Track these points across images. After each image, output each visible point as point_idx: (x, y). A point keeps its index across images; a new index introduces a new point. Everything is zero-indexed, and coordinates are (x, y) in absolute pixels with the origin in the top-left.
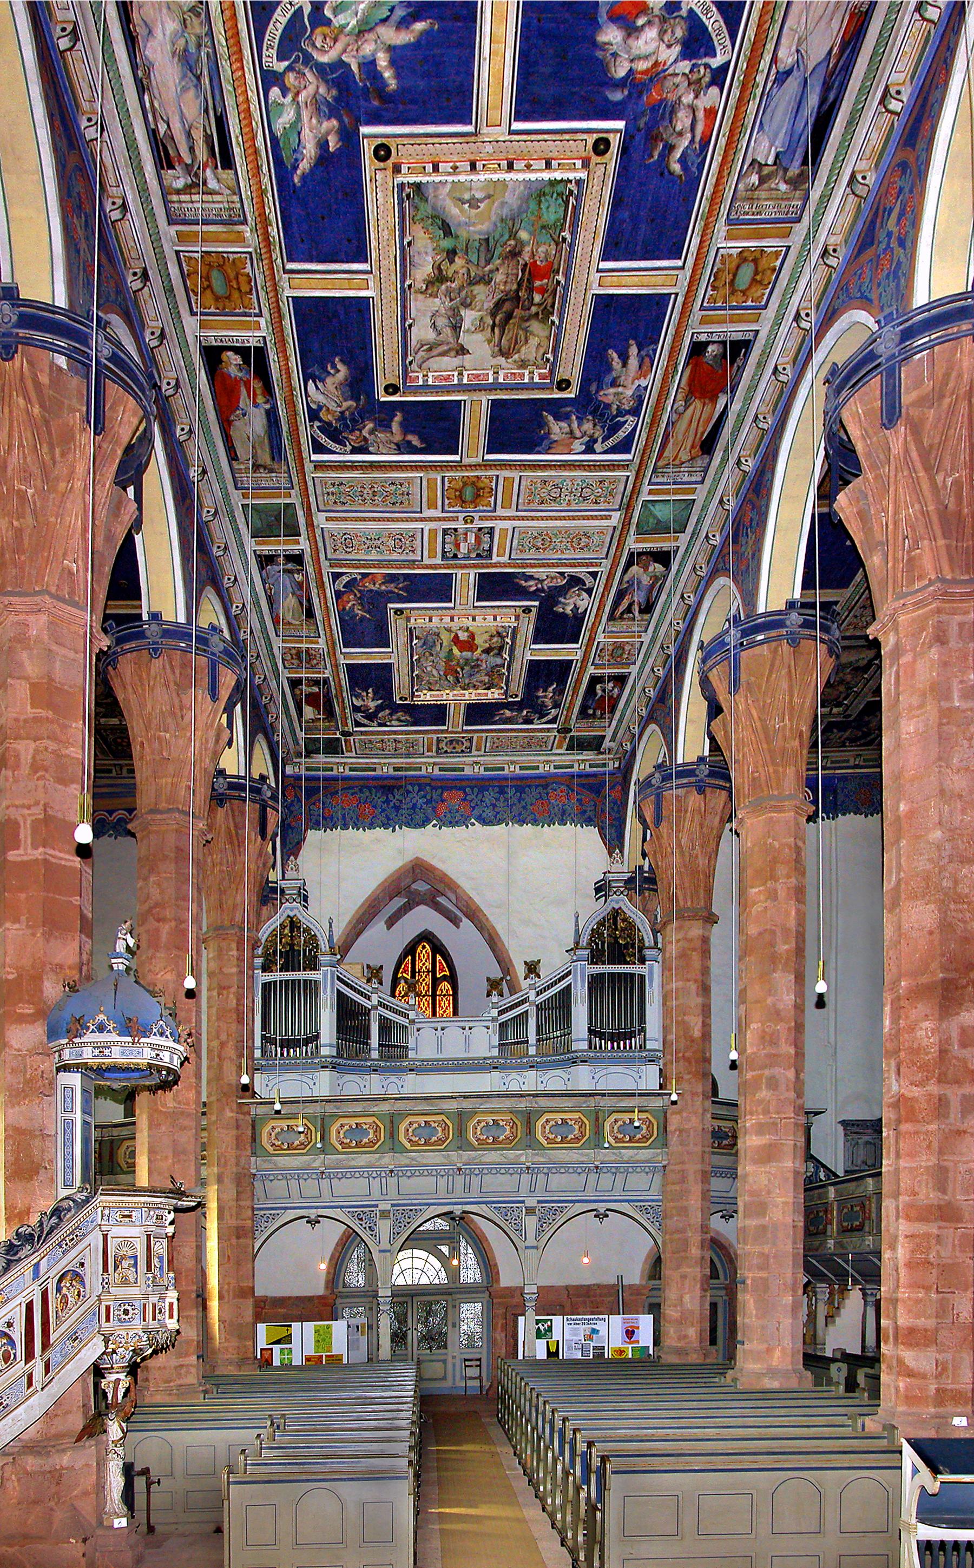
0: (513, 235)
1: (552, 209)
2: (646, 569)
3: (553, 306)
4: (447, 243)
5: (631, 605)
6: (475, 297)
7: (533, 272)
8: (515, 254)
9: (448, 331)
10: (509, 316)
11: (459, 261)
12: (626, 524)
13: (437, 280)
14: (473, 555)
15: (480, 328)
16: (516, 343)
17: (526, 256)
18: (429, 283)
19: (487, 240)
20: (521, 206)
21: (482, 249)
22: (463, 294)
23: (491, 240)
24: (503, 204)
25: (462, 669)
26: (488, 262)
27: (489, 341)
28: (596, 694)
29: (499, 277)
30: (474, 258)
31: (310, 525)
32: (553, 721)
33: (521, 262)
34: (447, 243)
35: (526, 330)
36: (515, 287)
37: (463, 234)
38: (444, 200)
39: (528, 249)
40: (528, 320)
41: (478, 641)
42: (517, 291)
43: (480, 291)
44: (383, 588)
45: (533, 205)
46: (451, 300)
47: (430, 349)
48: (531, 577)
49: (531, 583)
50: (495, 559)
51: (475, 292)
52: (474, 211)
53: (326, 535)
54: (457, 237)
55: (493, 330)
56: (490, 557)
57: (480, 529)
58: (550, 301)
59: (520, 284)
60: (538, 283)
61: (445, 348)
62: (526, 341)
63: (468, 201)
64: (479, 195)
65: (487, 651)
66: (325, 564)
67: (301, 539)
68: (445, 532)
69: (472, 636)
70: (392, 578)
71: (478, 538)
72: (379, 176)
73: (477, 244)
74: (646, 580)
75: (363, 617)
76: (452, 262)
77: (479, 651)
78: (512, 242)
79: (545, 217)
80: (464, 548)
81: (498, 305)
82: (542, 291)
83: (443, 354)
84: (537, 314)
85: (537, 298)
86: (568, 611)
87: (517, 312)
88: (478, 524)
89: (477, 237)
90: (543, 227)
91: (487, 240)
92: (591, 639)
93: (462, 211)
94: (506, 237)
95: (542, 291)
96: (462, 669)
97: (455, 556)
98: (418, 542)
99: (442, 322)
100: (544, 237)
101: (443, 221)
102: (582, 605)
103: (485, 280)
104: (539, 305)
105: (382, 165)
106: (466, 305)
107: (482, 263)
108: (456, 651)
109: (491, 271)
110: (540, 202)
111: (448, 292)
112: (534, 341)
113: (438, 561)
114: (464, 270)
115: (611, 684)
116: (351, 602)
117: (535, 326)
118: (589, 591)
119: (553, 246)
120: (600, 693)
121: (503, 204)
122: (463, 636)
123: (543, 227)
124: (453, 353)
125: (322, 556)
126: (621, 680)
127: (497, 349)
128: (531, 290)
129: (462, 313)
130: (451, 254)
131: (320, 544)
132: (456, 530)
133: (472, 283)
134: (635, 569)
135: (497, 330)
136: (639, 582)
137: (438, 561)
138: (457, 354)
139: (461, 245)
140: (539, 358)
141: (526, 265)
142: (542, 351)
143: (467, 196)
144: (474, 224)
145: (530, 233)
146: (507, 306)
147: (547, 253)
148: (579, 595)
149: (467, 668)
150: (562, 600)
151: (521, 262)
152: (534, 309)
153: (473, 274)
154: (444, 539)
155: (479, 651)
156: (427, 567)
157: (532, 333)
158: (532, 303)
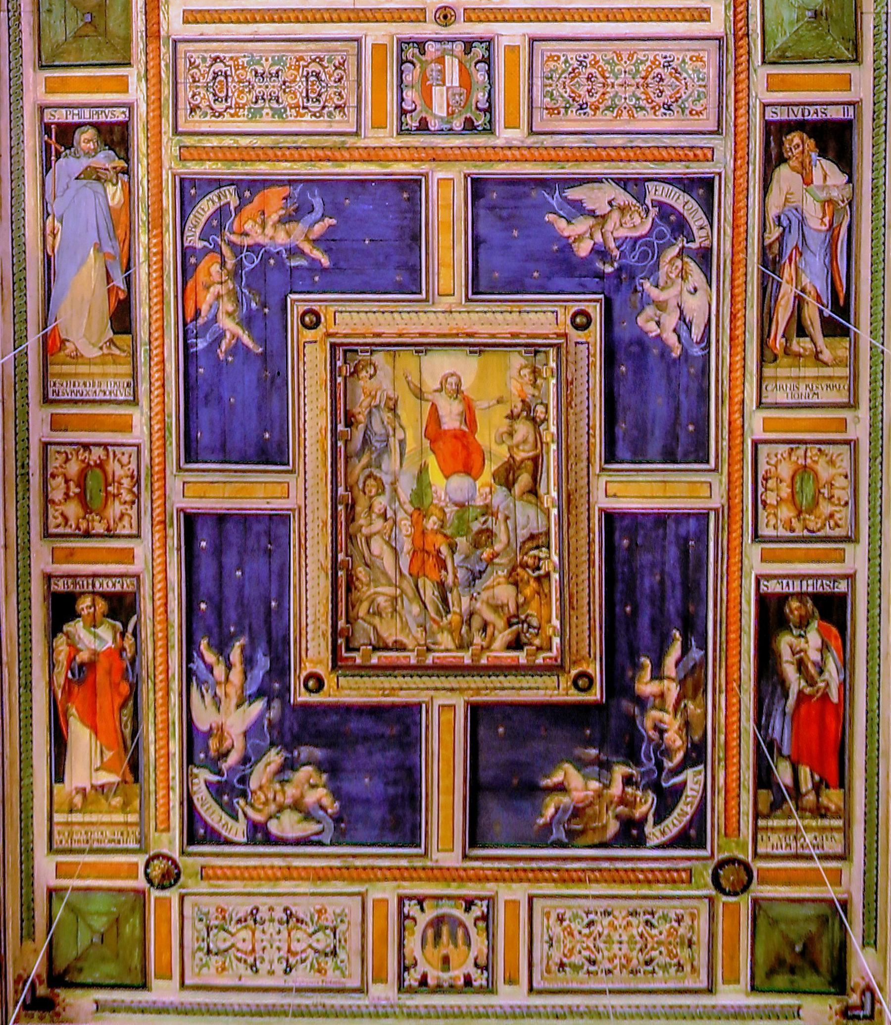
2: (808, 182)
5: (799, 302)
12: (741, 34)
14: (458, 124)
25: (453, 548)
28: (783, 683)
31: (153, 34)
32: (691, 836)
41: (485, 437)
44: (281, 238)
48: (578, 208)
49: (582, 225)
50: (505, 135)
53: (181, 63)
56: (489, 130)
57: (468, 45)
65: (507, 476)
66: (170, 147)
67: (133, 74)
68: (403, 43)
69: (469, 416)
70: (300, 200)
71: (464, 73)
74: (816, 221)
75: (238, 348)
77: (486, 476)
80: (439, 108)
86: (671, 339)
88: (462, 29)
92: (737, 430)
96: (453, 548)
97: (423, 127)
98: (349, 83)
102: (695, 306)
108: (435, 474)
113: (388, 137)
115: (814, 638)
116: (215, 294)
118: (704, 257)
120: (790, 671)
122: (451, 420)
125: (167, 126)
126: (832, 608)
131: (167, 91)
132: (421, 44)
134: (785, 175)
136: (802, 222)
137: (388, 137)
148: (683, 275)
149: (462, 542)
150: (654, 293)
154: (401, 73)
155: (486, 476)
156: (370, 155)
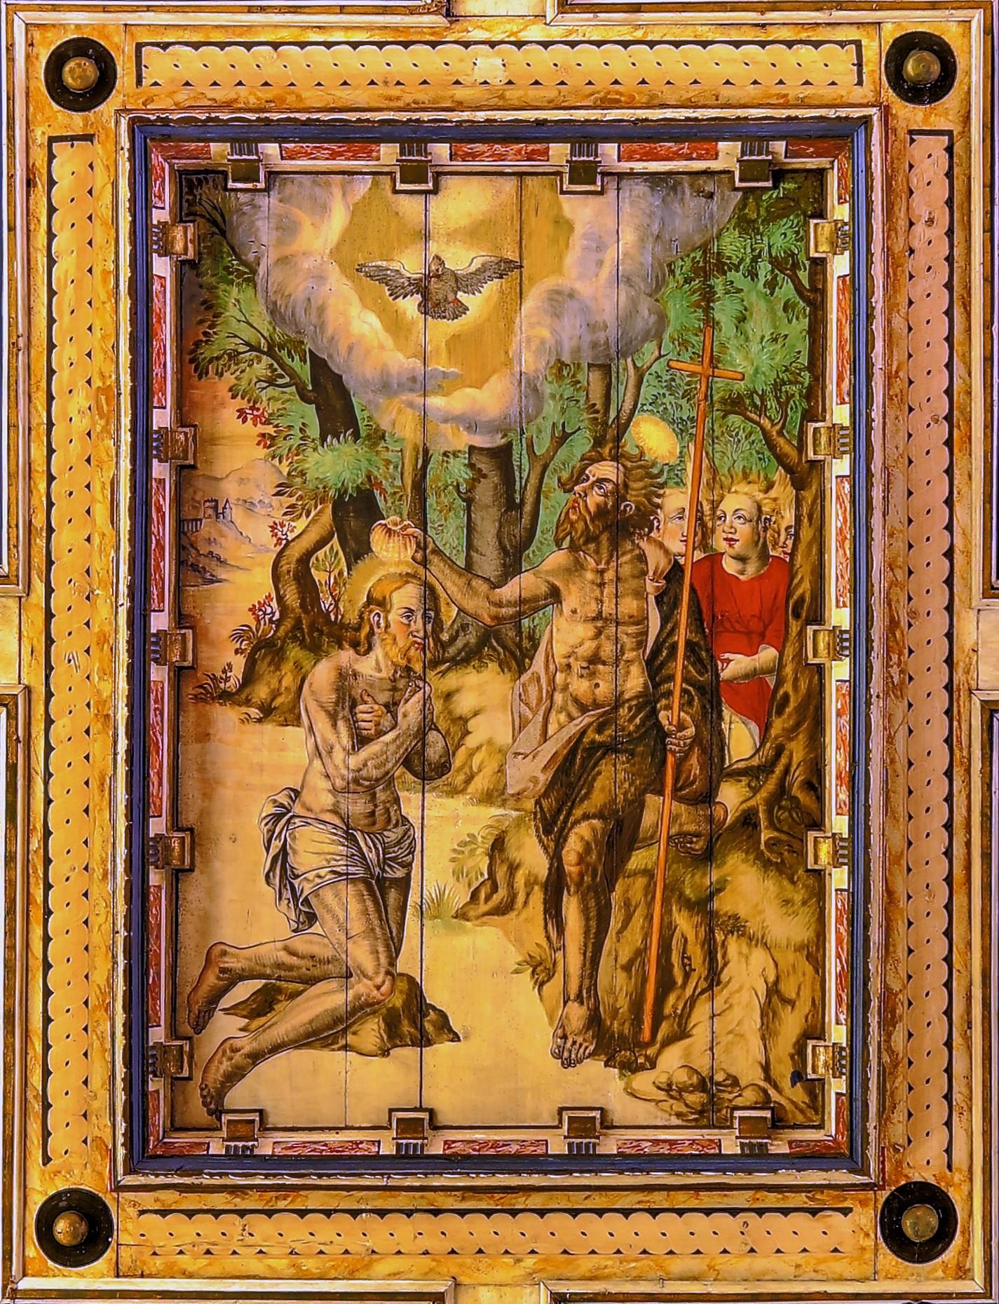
0: (610, 436)
1: (759, 325)
3: (815, 784)
4: (334, 464)
6: (464, 720)
7: (703, 607)
8: (621, 524)
9: (345, 908)
10: (621, 834)
11: (390, 551)
13: (296, 633)
15: (492, 897)
16: (666, 985)
17: (672, 537)
18: (264, 650)
19: (502, 456)
20: (626, 318)
21: (485, 492)
22: (411, 710)
23: (520, 457)
24: (559, 300)
26: (512, 568)
27: (541, 971)
29: (566, 634)
30: (449, 534)
33: (656, 560)
34: (334, 464)
35: (703, 906)
36: (635, 681)
37: (399, 420)
38: (321, 278)
39: (675, 500)
40: (708, 857)
42: (649, 702)
43: (481, 691)
45: (679, 311)
46: (361, 740)
47: (263, 1004)
51: (464, 704)
52: (442, 329)
54: (378, 436)
55: (553, 910)
58: (797, 750)
59: (655, 667)
60: (736, 665)
61: (326, 1000)
62: (714, 978)
63: (421, 287)
64: (460, 259)
72: (67, 164)
73: (459, 471)
76: (358, 551)
78: (606, 470)
79: (738, 361)
81: (570, 774)
82: (761, 700)
83: (329, 1034)
84: (748, 820)
85: (741, 739)
87: (659, 812)
89: (463, 440)
90: (735, 404)
91: (502, 456)
93: (395, 325)
94: (581, 444)
95: (761, 700)
99: (315, 850)
100: (738, 445)
101: (319, 365)
103: (508, 643)
104: (753, 774)
105: (76, 121)
106: (427, 768)
107: (489, 563)
109: (528, 606)
110: (708, 296)
111: (346, 698)
112: (747, 971)
114: (406, 597)
117: (747, 887)
119: (783, 491)
121: (559, 300)
123: (735, 404)
124: (370, 1032)
127: (577, 1014)
128: (710, 697)
129: (410, 805)
130: (355, 514)
133: (446, 649)
135: (571, 908)
138: (393, 1037)
139: (394, 486)
140: (783, 1071)
141: (676, 571)
142: (791, 1024)
143: (410, 264)
144: (445, 384)
145: (681, 428)
146: (610, 780)
147: (760, 520)
151: (656, 560)
152: (731, 796)
153: (449, 614)
157: (736, 926)
158: (717, 771)
